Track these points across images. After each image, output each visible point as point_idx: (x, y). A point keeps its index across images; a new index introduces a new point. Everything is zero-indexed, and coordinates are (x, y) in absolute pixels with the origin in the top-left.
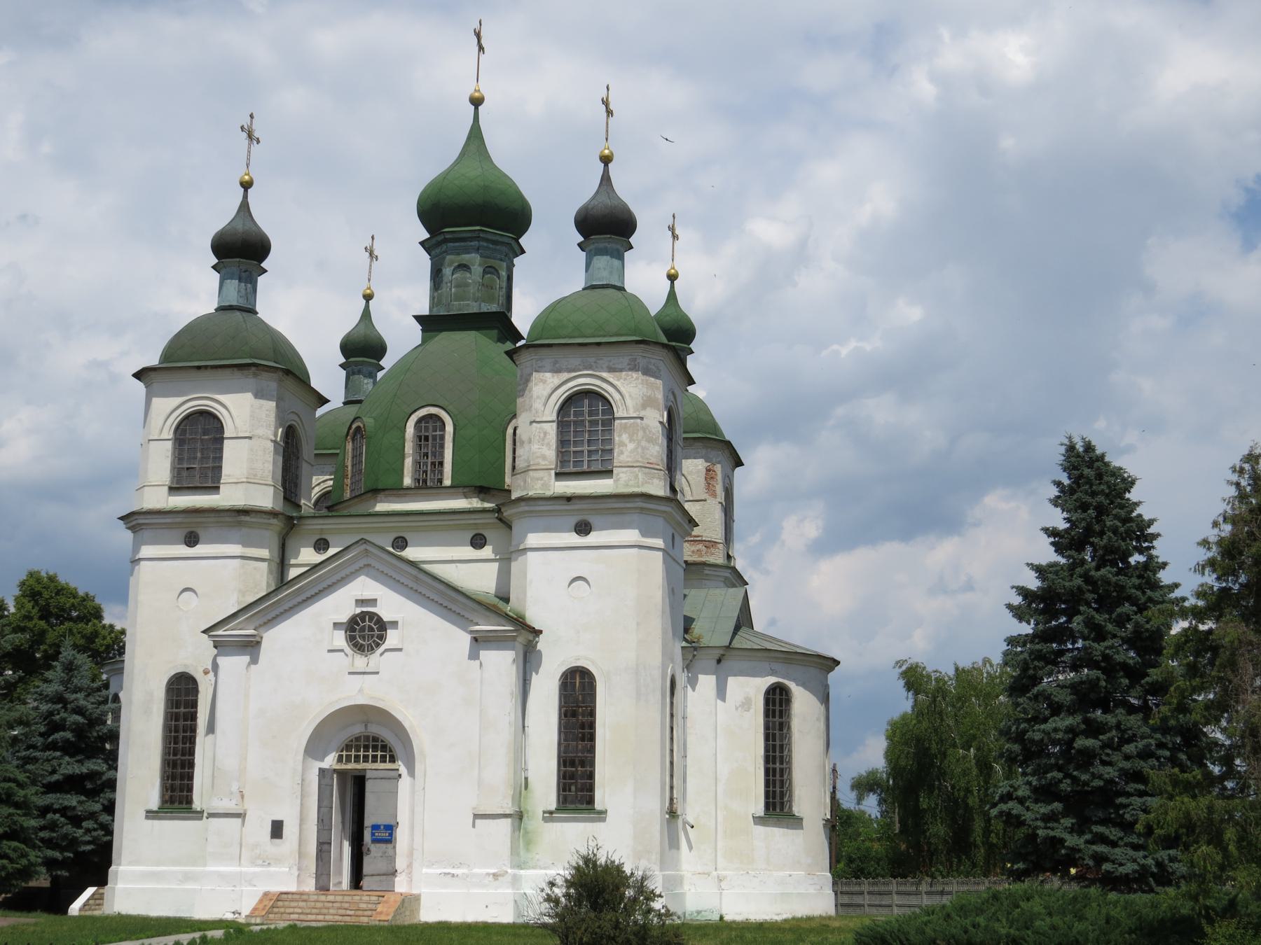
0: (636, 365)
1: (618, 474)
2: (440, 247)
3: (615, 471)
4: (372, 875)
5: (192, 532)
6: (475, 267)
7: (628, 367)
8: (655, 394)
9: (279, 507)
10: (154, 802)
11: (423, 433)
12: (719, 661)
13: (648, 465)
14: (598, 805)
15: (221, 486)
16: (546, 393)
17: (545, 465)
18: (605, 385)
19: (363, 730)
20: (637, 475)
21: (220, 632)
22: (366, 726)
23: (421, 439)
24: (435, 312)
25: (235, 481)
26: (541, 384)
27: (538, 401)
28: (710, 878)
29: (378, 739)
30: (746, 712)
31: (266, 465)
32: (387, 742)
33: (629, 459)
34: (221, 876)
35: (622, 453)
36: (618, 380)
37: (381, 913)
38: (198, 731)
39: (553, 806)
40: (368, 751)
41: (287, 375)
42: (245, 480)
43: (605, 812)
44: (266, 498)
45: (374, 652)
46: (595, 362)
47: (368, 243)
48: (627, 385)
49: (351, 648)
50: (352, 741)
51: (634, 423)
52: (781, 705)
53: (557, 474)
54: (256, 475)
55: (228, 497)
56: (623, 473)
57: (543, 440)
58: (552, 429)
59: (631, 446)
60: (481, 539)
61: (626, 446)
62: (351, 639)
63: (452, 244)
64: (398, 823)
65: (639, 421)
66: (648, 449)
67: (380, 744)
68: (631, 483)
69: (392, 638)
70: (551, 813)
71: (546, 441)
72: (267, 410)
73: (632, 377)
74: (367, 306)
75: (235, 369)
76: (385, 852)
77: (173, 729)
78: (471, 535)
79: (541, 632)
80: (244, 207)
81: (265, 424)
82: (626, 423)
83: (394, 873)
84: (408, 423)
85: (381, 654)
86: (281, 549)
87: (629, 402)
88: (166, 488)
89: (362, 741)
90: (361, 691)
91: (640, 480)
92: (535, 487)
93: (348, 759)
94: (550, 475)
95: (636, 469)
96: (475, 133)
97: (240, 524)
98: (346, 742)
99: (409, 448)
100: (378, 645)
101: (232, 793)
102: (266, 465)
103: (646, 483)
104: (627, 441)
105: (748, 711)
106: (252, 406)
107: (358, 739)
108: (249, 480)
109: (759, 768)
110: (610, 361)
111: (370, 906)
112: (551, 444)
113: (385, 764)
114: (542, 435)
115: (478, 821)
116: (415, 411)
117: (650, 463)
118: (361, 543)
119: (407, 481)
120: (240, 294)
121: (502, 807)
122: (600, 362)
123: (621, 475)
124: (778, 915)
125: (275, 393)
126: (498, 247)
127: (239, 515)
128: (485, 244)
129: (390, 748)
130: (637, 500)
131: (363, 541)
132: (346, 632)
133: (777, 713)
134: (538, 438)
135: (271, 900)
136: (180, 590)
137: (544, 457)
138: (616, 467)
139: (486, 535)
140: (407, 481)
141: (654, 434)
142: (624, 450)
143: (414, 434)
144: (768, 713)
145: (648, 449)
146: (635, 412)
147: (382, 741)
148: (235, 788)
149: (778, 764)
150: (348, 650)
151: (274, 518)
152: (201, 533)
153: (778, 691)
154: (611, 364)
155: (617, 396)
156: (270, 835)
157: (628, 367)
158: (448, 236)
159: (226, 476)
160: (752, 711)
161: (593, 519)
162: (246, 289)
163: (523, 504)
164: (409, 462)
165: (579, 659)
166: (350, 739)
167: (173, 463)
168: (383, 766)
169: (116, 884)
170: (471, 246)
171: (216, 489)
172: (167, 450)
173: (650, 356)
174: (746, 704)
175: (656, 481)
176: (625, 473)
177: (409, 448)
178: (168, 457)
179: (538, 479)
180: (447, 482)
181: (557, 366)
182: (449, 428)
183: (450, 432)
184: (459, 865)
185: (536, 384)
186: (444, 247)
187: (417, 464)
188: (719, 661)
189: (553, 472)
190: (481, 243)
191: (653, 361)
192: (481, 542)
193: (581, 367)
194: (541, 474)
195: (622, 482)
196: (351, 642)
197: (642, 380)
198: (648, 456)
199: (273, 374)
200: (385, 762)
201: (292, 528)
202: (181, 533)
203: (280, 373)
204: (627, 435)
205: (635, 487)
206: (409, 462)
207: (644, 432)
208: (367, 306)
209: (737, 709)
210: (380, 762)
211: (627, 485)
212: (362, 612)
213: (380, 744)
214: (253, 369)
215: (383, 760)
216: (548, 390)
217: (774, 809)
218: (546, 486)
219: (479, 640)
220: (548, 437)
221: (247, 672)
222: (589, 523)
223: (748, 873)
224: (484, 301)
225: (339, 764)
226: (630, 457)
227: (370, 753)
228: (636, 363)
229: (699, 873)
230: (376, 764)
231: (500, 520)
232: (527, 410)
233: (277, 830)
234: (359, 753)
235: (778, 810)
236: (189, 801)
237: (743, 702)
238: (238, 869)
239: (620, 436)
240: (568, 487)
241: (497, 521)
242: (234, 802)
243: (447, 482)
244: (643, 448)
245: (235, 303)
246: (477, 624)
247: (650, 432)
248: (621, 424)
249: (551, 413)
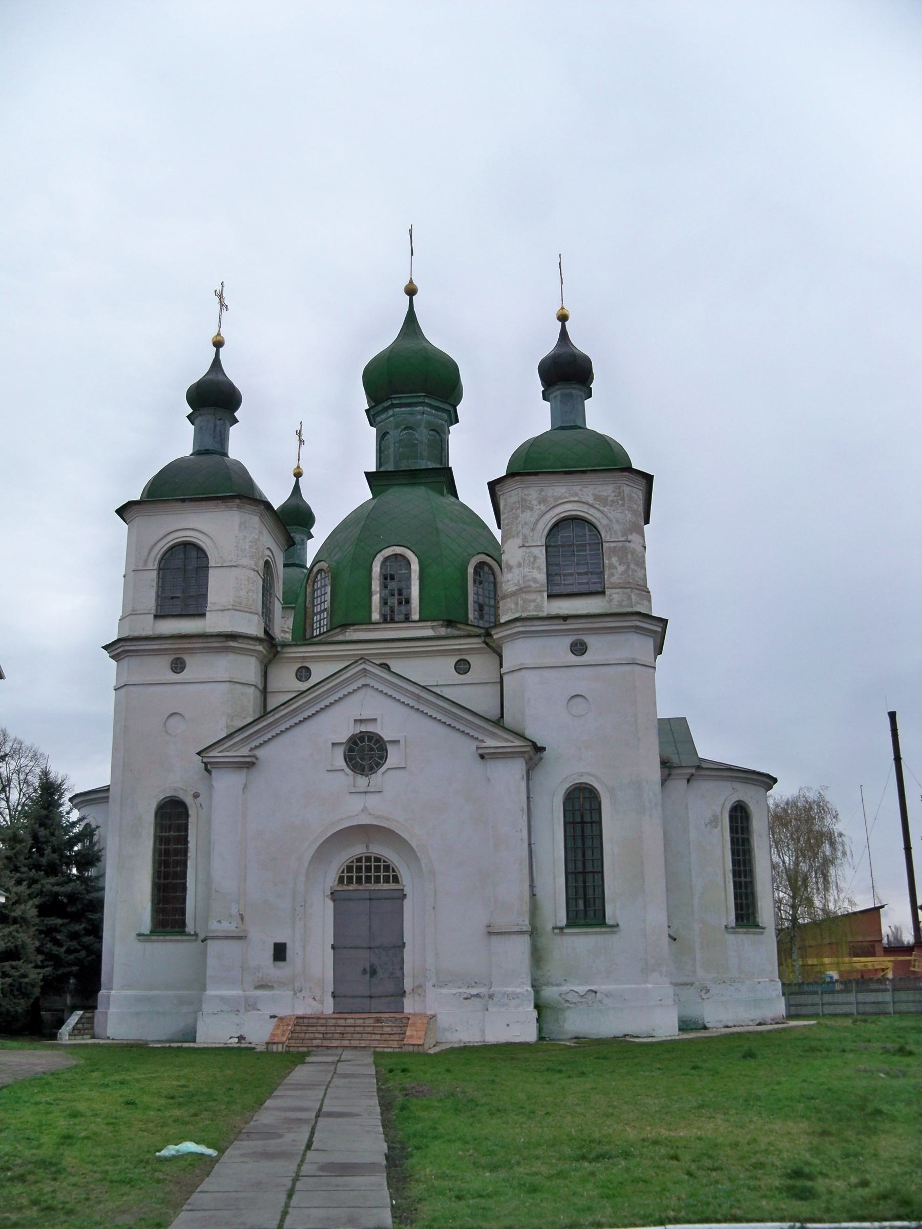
0: (620, 493)
1: (611, 595)
2: (386, 413)
3: (608, 592)
4: (380, 997)
5: (177, 659)
6: (422, 429)
7: (613, 494)
8: (638, 521)
9: (261, 634)
10: (146, 925)
11: (389, 571)
12: (688, 781)
13: (638, 587)
14: (609, 919)
15: (208, 614)
16: (533, 520)
17: (537, 587)
18: (592, 511)
19: (365, 851)
20: (630, 596)
21: (215, 753)
22: (367, 847)
23: (386, 578)
24: (382, 469)
25: (221, 608)
26: (529, 511)
27: (527, 527)
28: (693, 988)
29: (380, 859)
30: (714, 829)
31: (250, 594)
32: (389, 863)
33: (621, 581)
34: (222, 999)
35: (613, 575)
36: (604, 507)
37: (411, 1037)
38: (189, 855)
39: (563, 922)
40: (380, 872)
41: (267, 510)
42: (231, 607)
43: (617, 926)
44: (252, 626)
45: (376, 772)
46: (581, 490)
47: (298, 428)
48: (614, 511)
49: (351, 769)
50: (352, 862)
51: (622, 547)
52: (742, 823)
53: (549, 596)
54: (240, 603)
55: (213, 623)
56: (616, 593)
57: (533, 564)
58: (541, 553)
59: (621, 568)
60: (465, 664)
61: (616, 569)
62: (349, 758)
63: (398, 409)
64: (404, 943)
65: (627, 544)
66: (636, 572)
67: (382, 864)
68: (625, 603)
69: (393, 757)
70: (561, 929)
71: (536, 565)
72: (250, 542)
73: (618, 504)
74: (297, 482)
75: (219, 502)
76: (392, 973)
77: (163, 852)
78: (457, 659)
79: (544, 749)
81: (248, 555)
82: (615, 547)
83: (403, 994)
84: (374, 563)
85: (383, 773)
86: (263, 678)
87: (616, 527)
88: (152, 616)
89: (364, 861)
90: (364, 809)
91: (634, 600)
92: (529, 608)
93: (350, 880)
94: (543, 597)
95: (629, 590)
96: (411, 318)
97: (228, 649)
98: (346, 864)
99: (376, 586)
100: (379, 765)
101: (231, 916)
102: (250, 594)
104: (617, 564)
105: (716, 827)
106: (236, 537)
107: (359, 860)
108: (236, 608)
109: (729, 882)
110: (595, 489)
111: (395, 1029)
112: (541, 568)
113: (388, 885)
114: (532, 559)
115: (494, 939)
116: (381, 551)
117: (639, 585)
118: (360, 662)
119: (376, 616)
121: (518, 925)
122: (585, 489)
123: (614, 596)
124: (752, 1020)
125: (257, 526)
126: (439, 413)
127: (227, 641)
128: (429, 410)
129: (393, 869)
130: (634, 618)
131: (363, 661)
132: (345, 753)
133: (740, 830)
134: (527, 562)
135: (288, 1025)
136: (166, 717)
137: (535, 580)
138: (608, 588)
139: (469, 661)
140: (376, 616)
142: (615, 572)
143: (381, 572)
144: (733, 830)
145: (636, 572)
146: (622, 536)
147: (384, 861)
148: (234, 911)
149: (743, 878)
150: (347, 770)
151: (260, 645)
152: (188, 659)
153: (739, 809)
154: (596, 492)
155: (605, 521)
156: (272, 958)
157: (613, 494)
158: (395, 402)
159: (211, 603)
160: (719, 827)
161: (590, 640)
162: (221, 436)
163: (518, 624)
164: (376, 599)
165: (582, 776)
166: (351, 860)
167: (157, 592)
168: (386, 886)
169: (108, 1008)
170: (416, 410)
171: (203, 615)
172: (152, 580)
173: (632, 485)
174: (714, 821)
176: (618, 593)
177: (376, 586)
178: (153, 586)
179: (531, 601)
180: (416, 617)
181: (543, 493)
182: (415, 567)
183: (415, 571)
184: (474, 984)
185: (523, 512)
186: (391, 412)
187: (384, 602)
188: (688, 781)
189: (545, 594)
190: (425, 408)
191: (634, 490)
192: (465, 666)
193: (567, 495)
194: (533, 596)
195: (615, 602)
196: (350, 762)
197: (628, 507)
198: (637, 579)
199: (254, 507)
200: (388, 882)
201: (275, 656)
202: (166, 661)
203: (263, 507)
204: (616, 558)
205: (627, 606)
206: (376, 599)
207: (632, 555)
208: (297, 482)
209: (706, 825)
210: (384, 883)
211: (621, 605)
212: (361, 732)
213: (382, 864)
214: (238, 501)
215: (387, 880)
216: (537, 517)
217: (742, 921)
218: (539, 607)
219: (486, 757)
220: (538, 561)
221: (244, 793)
222: (585, 644)
223: (724, 982)
224: (429, 460)
225: (341, 885)
226: (621, 578)
227: (373, 874)
228: (621, 490)
229: (682, 984)
230: (379, 884)
231: (487, 644)
232: (514, 537)
233: (280, 952)
234: (360, 874)
235: (745, 921)
236: (183, 924)
237: (711, 820)
238: (240, 992)
239: (609, 559)
240: (559, 608)
241: (484, 646)
242: (234, 925)
243: (416, 617)
244: (633, 571)
245: (211, 448)
246: (483, 741)
247: (637, 555)
248: (610, 548)
249: (539, 537)
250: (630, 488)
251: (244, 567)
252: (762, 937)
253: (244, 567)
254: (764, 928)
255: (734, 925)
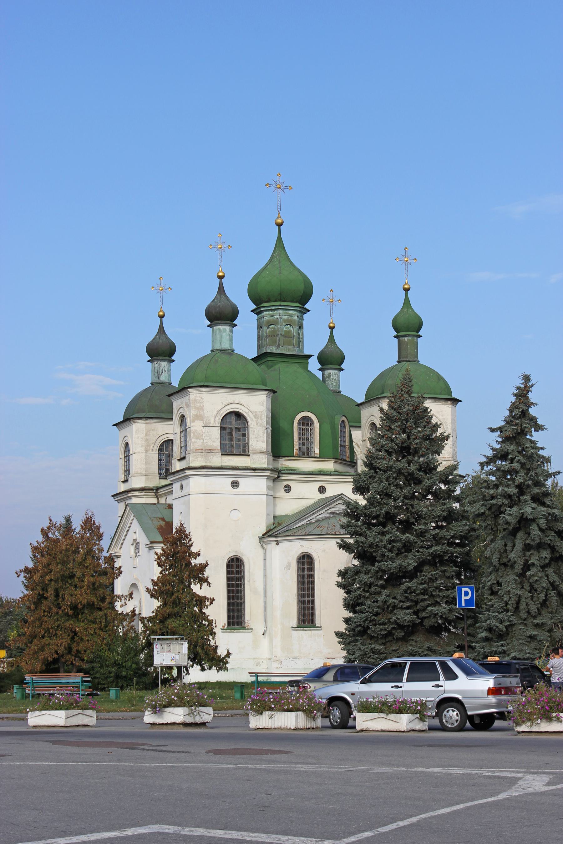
8: (200, 412)
54: (138, 472)
80: (161, 329)
103: (194, 461)
117: (197, 450)
120: (155, 376)
125: (145, 429)
128: (267, 313)
141: (200, 434)
145: (196, 443)
174: (288, 566)
175: (200, 459)
191: (197, 395)
235: (307, 623)
247: (197, 433)
250: (195, 395)
251: (139, 453)
252: (321, 632)
253: (139, 453)
254: (321, 627)
255: (296, 626)
